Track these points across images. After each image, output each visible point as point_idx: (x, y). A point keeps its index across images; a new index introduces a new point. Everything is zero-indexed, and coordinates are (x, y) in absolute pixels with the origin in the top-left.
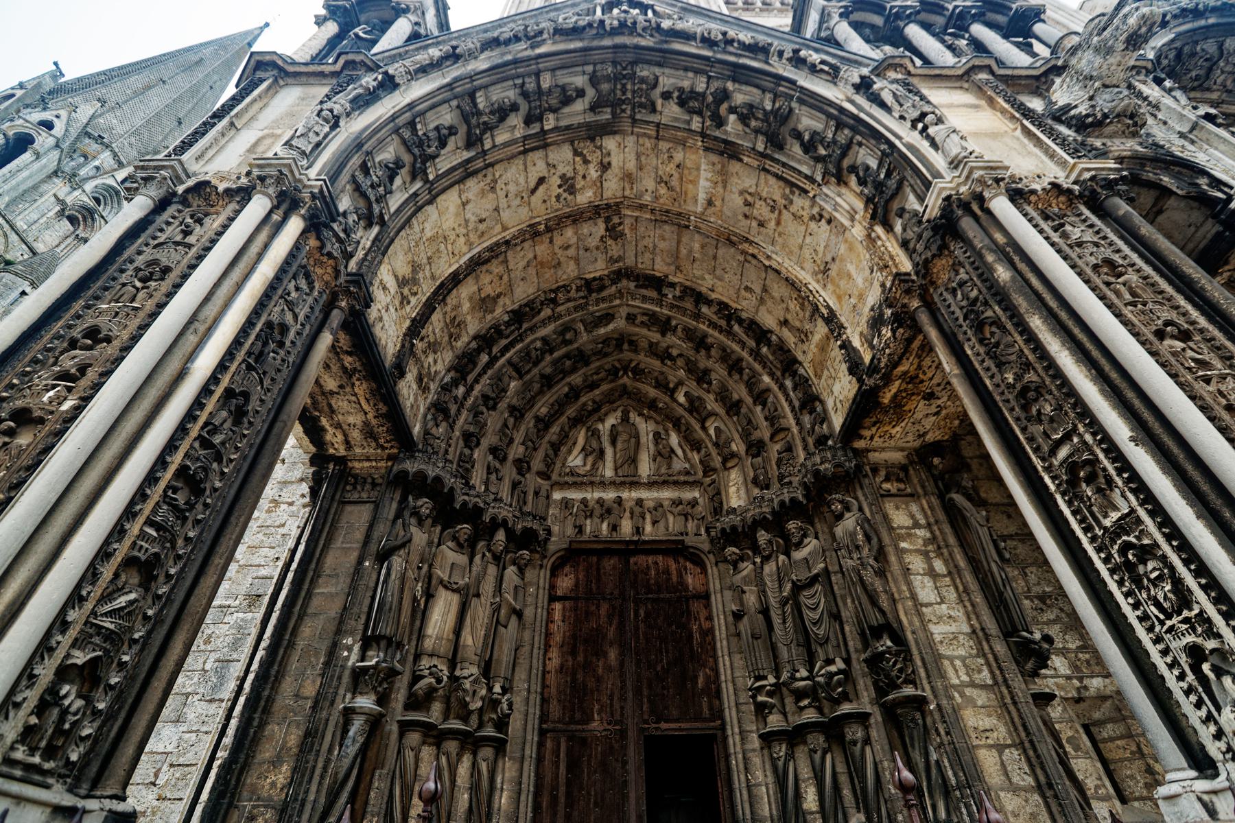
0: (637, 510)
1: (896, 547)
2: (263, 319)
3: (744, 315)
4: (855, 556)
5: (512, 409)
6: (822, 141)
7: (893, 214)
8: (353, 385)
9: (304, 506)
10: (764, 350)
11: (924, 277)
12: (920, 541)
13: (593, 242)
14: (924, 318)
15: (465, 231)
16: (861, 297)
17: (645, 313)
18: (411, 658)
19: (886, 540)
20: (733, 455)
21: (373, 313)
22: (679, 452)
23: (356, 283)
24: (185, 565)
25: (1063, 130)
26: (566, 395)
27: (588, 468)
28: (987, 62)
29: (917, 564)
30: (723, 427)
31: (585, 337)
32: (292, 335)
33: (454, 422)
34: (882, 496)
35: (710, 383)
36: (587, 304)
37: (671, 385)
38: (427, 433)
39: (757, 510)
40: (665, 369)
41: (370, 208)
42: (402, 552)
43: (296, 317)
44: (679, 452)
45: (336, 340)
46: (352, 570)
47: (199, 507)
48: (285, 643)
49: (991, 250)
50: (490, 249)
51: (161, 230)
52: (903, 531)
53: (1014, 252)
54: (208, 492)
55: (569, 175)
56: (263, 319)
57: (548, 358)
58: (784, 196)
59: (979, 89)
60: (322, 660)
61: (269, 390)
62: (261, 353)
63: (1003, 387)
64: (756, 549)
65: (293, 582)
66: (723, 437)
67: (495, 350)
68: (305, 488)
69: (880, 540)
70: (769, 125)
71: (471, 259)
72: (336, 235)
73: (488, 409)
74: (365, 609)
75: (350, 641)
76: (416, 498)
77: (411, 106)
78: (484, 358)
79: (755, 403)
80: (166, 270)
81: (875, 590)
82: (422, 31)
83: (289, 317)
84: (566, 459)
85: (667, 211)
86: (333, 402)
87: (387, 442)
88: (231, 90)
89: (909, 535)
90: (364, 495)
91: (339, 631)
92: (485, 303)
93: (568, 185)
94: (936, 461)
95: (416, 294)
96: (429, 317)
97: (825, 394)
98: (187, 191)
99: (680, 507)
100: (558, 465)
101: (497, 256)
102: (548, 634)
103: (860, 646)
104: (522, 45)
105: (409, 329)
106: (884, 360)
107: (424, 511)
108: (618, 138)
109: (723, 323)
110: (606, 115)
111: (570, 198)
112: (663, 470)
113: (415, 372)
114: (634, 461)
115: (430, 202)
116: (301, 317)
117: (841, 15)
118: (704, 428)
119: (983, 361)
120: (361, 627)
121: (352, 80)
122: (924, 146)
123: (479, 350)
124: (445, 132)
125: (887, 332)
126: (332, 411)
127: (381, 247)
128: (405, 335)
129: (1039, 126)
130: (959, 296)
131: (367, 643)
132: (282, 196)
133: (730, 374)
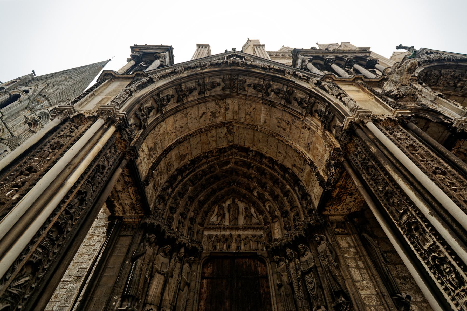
0: (238, 239)
1: (343, 256)
2: (96, 164)
3: (279, 162)
4: (327, 260)
5: (190, 198)
6: (305, 101)
7: (332, 127)
8: (128, 188)
9: (104, 237)
10: (287, 175)
11: (345, 150)
12: (352, 253)
13: (222, 135)
14: (346, 165)
15: (175, 131)
16: (322, 156)
17: (242, 161)
18: (142, 305)
19: (339, 253)
20: (276, 217)
21: (138, 161)
22: (255, 215)
23: (133, 150)
24: (51, 264)
25: (389, 99)
26: (211, 192)
27: (219, 221)
28: (360, 77)
29: (352, 263)
30: (272, 205)
31: (218, 170)
32: (107, 169)
33: (167, 203)
34: (336, 234)
35: (266, 188)
36: (220, 158)
37: (251, 189)
38: (155, 207)
39: (286, 240)
40: (249, 182)
41: (140, 123)
42: (142, 258)
43: (109, 163)
44: (255, 215)
45: (123, 171)
46: (120, 265)
47: (61, 239)
48: (89, 298)
49: (369, 141)
50: (184, 137)
51: (62, 131)
52: (345, 249)
53: (377, 142)
54: (65, 233)
55: (214, 112)
56: (96, 164)
57: (204, 178)
58: (292, 120)
59: (359, 86)
60: (103, 307)
61: (95, 191)
62: (94, 176)
63: (378, 192)
64: (286, 257)
65: (95, 271)
66: (272, 209)
67: (184, 175)
68: (105, 230)
69: (336, 253)
70: (286, 96)
71: (177, 141)
72: (127, 133)
73: (180, 198)
74: (124, 283)
75: (116, 298)
76: (149, 234)
77: (158, 88)
78: (180, 178)
79: (284, 196)
80: (62, 145)
81: (336, 275)
82: (164, 64)
83: (106, 163)
84: (210, 218)
85: (250, 125)
86: (120, 195)
87: (140, 211)
88: (94, 82)
89: (348, 251)
90: (129, 233)
91: (112, 293)
92: (181, 157)
93: (214, 115)
94: (356, 220)
95: (155, 154)
96: (159, 162)
97: (311, 193)
98: (74, 117)
99: (255, 238)
100: (207, 220)
101: (186, 140)
102: (200, 294)
103: (331, 300)
104: (199, 69)
105: (151, 167)
106: (332, 180)
107: (152, 240)
108: (232, 99)
109: (271, 165)
110: (228, 92)
111: (214, 119)
112: (248, 223)
113: (153, 183)
114: (237, 219)
115: (163, 121)
116: (111, 163)
117: (309, 61)
118: (265, 206)
119: (370, 182)
120: (122, 291)
121: (138, 80)
122: (341, 104)
123: (177, 175)
124: (170, 97)
125: (333, 170)
126: (119, 198)
127: (143, 137)
128: (150, 169)
129: (381, 98)
130: (358, 157)
131: (124, 298)
132: (108, 119)
133: (274, 185)
